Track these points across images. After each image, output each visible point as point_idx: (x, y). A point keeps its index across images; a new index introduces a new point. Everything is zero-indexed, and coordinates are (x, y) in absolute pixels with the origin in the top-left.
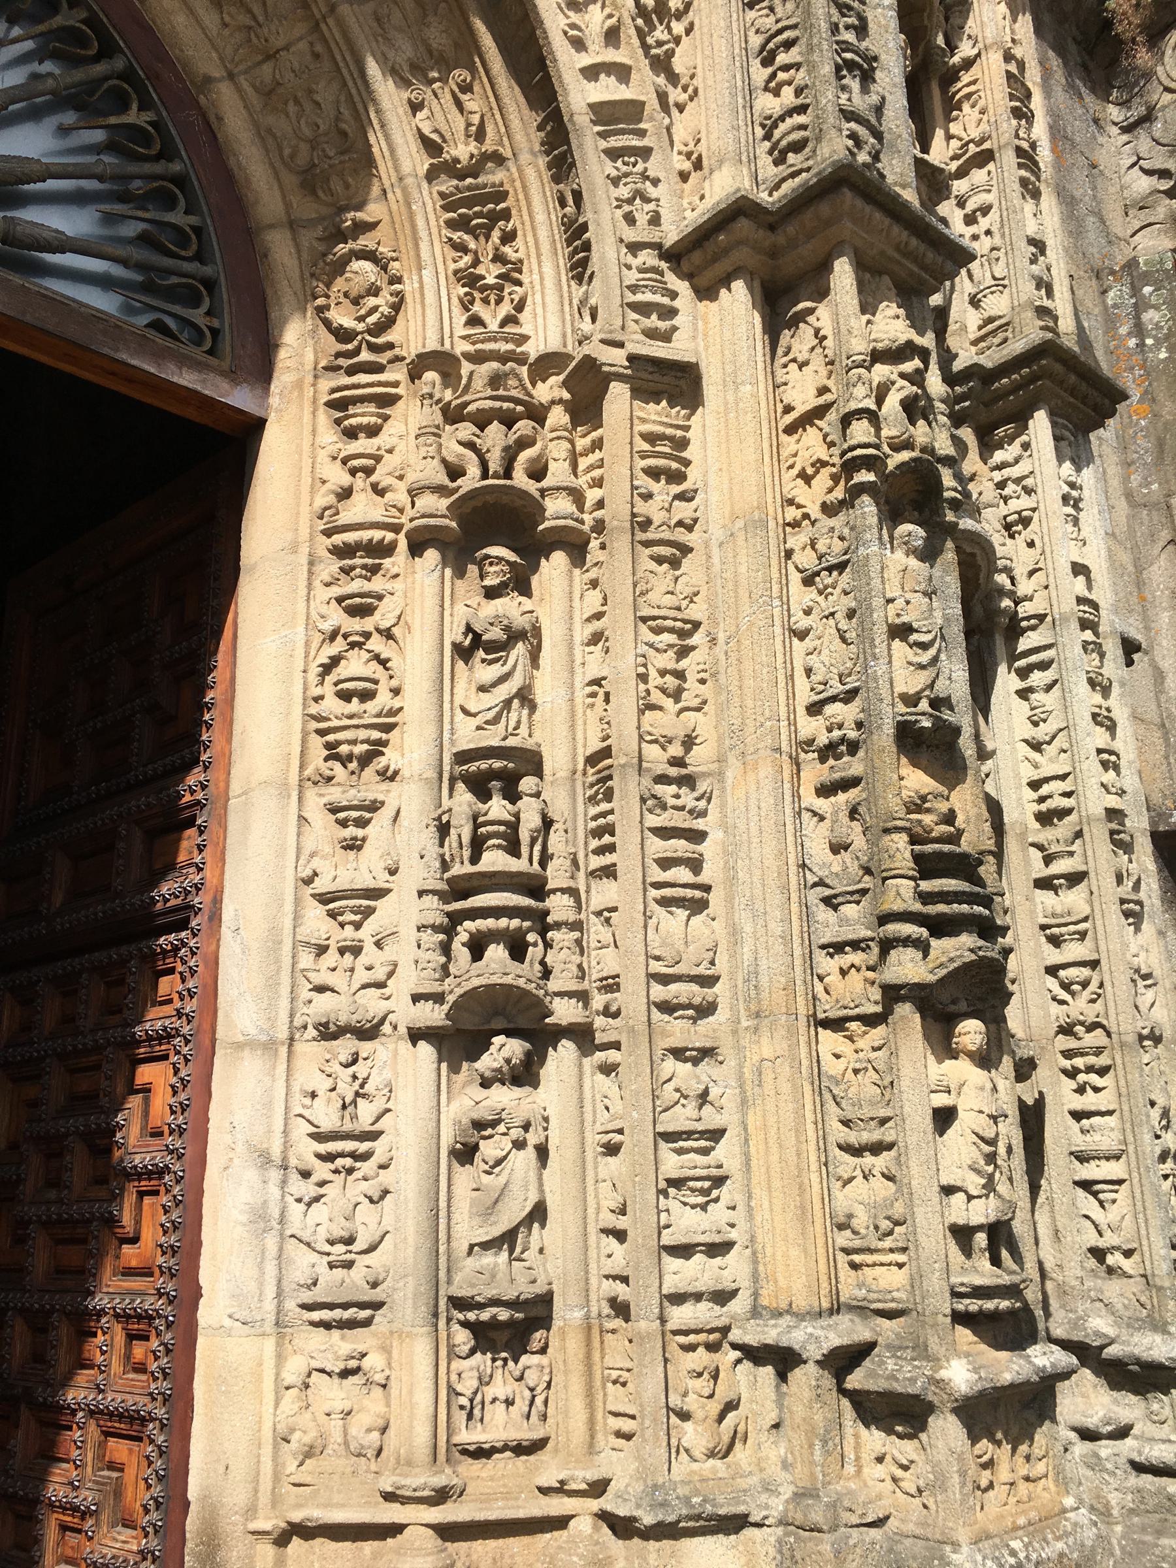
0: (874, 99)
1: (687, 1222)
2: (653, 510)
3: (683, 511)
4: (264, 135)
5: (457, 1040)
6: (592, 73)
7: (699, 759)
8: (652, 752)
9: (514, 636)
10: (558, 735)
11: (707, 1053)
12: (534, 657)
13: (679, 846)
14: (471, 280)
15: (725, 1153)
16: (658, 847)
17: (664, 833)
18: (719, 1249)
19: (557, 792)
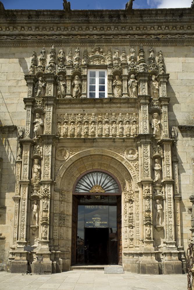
0: (148, 172)
1: (137, 235)
2: (137, 199)
3: (138, 199)
4: (120, 179)
5: (129, 227)
6: (133, 174)
7: (139, 213)
8: (136, 212)
9: (131, 207)
10: (134, 212)
11: (139, 227)
12: (133, 207)
13: (138, 217)
14: (129, 186)
15: (139, 232)
16: (136, 217)
17: (137, 217)
18: (139, 236)
19: (134, 215)
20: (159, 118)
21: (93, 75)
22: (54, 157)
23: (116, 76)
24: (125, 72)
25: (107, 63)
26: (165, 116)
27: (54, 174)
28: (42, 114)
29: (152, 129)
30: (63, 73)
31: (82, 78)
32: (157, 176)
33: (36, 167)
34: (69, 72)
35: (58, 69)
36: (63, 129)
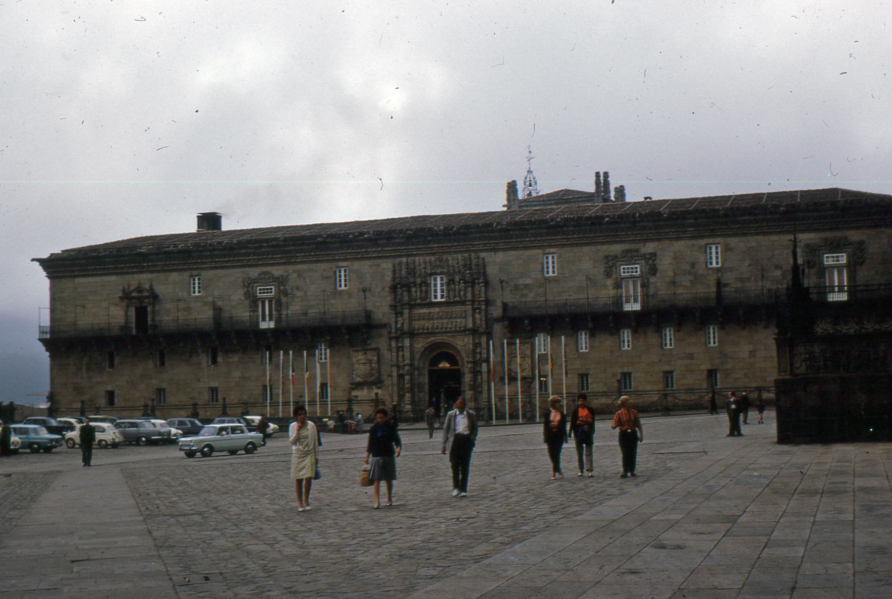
20: (480, 313)
21: (435, 280)
22: (411, 346)
23: (451, 282)
24: (457, 278)
25: (445, 271)
26: (483, 314)
27: (412, 358)
28: (402, 314)
29: (474, 322)
30: (414, 283)
31: (428, 285)
32: (478, 356)
33: (401, 353)
34: (419, 281)
35: (411, 280)
36: (417, 324)
